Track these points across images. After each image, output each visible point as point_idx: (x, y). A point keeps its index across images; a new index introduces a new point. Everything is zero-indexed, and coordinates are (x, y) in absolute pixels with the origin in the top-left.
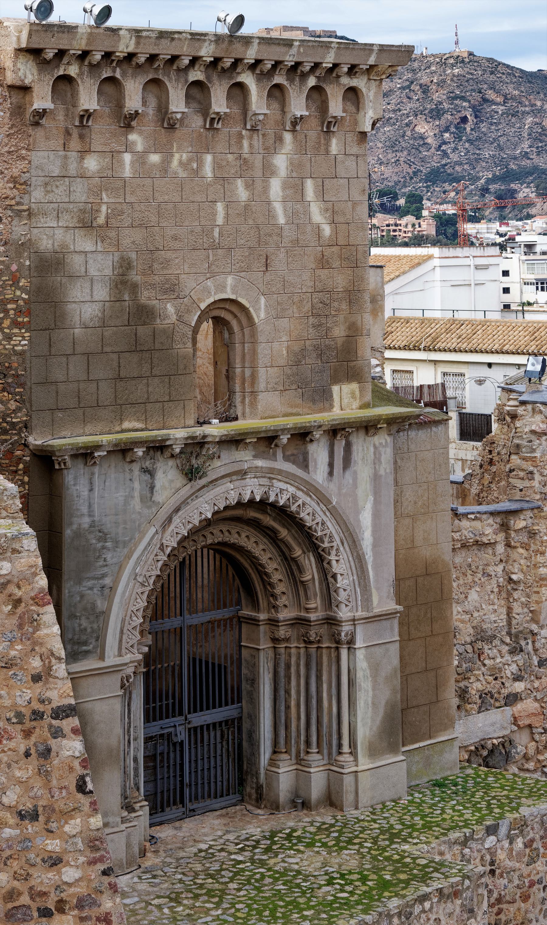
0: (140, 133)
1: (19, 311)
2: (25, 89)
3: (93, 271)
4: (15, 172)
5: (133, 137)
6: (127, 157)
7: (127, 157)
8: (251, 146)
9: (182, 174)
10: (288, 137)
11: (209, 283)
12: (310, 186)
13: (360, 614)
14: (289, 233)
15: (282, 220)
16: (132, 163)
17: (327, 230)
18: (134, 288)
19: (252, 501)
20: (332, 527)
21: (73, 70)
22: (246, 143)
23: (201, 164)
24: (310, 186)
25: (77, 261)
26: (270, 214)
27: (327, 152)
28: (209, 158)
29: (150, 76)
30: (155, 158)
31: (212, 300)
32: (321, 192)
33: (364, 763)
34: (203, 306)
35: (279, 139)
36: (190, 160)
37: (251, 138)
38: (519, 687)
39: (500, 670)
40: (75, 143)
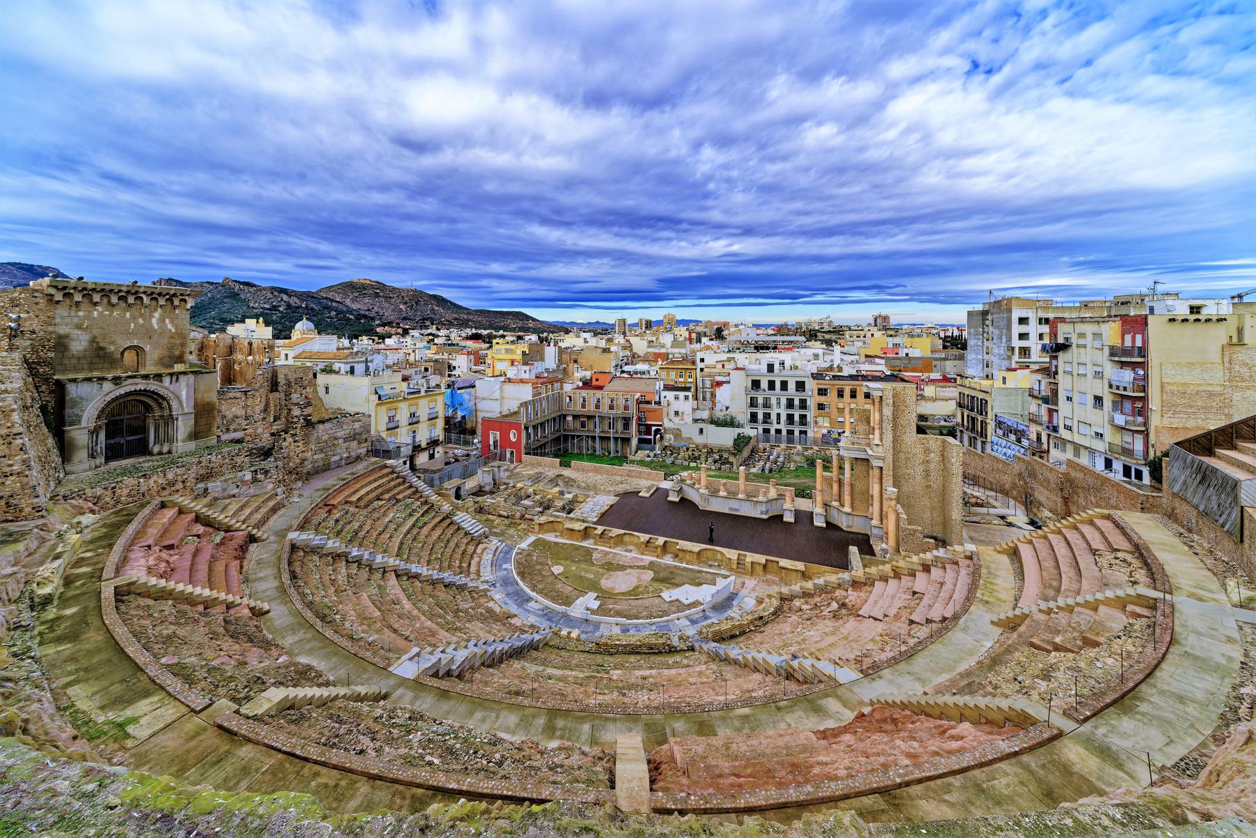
3: (81, 338)
12: (167, 321)
14: (159, 331)
18: (98, 343)
20: (170, 395)
24: (167, 321)
25: (75, 337)
26: (152, 326)
32: (172, 322)
33: (180, 444)
40: (74, 308)
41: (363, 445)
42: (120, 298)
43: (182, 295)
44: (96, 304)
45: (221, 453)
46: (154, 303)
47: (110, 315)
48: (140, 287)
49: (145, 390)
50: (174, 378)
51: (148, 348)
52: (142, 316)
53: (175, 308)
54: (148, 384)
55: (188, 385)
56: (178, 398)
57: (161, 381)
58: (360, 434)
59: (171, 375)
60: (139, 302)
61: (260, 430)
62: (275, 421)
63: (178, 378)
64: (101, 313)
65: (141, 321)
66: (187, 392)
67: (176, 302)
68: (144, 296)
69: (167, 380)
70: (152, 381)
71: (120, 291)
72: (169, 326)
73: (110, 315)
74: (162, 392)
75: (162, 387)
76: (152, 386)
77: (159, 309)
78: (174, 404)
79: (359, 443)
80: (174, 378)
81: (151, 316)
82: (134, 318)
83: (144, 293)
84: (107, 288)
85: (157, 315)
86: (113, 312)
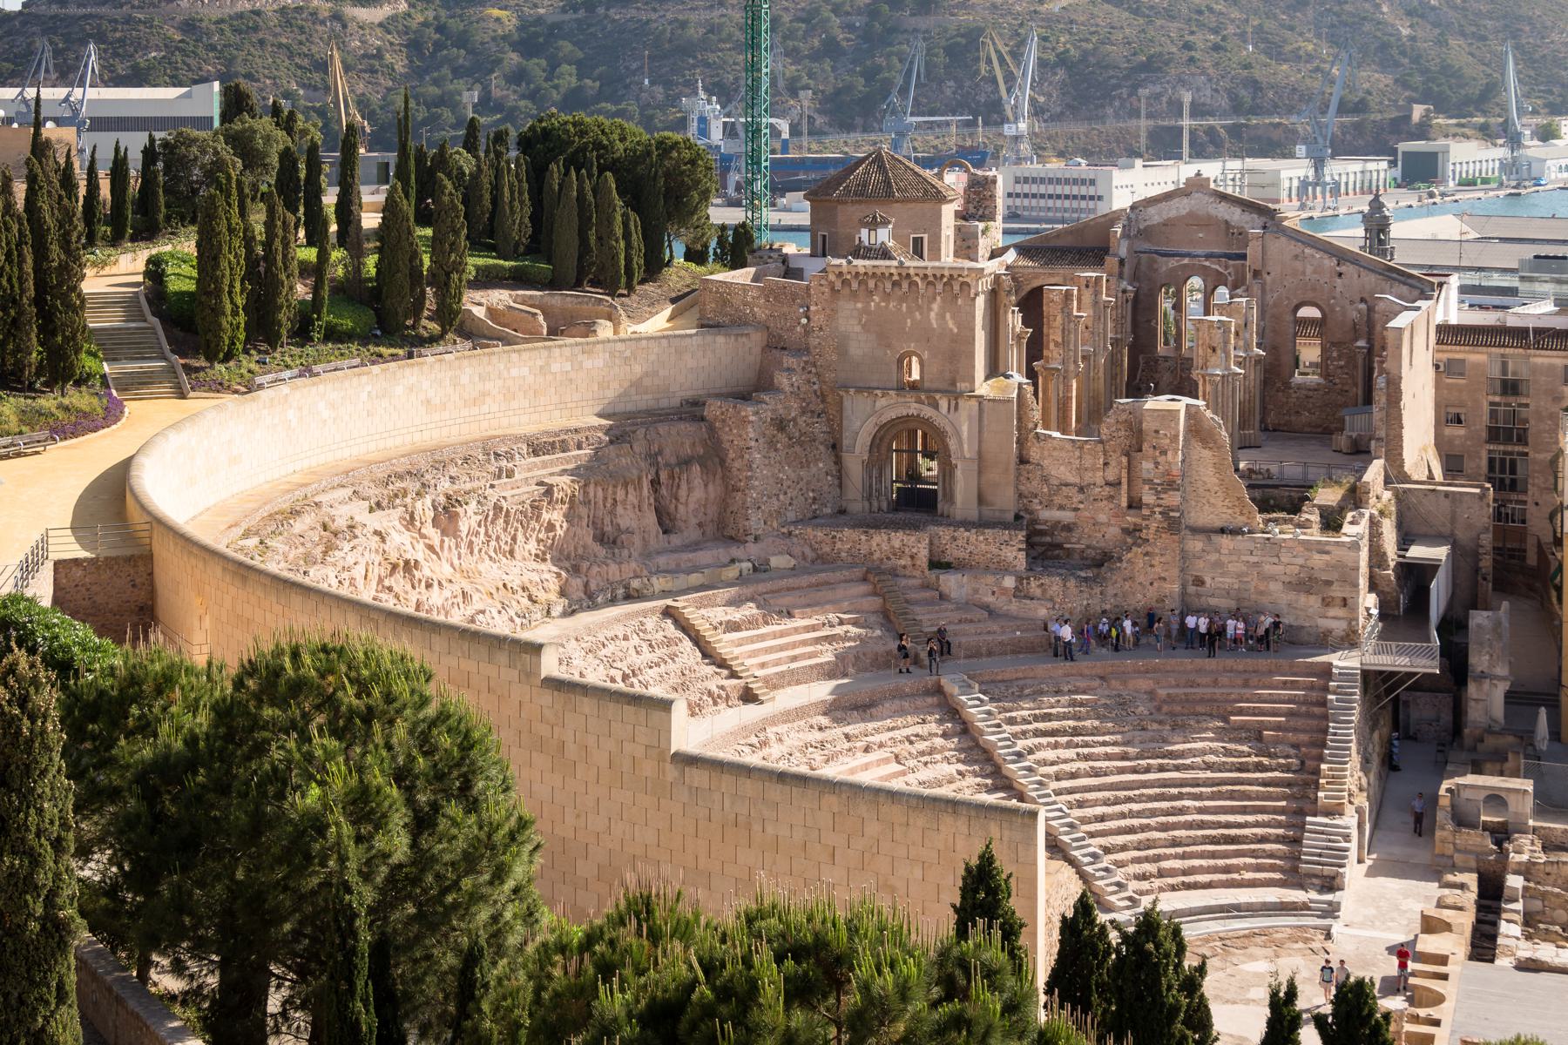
10: (938, 298)
12: (948, 316)
17: (956, 330)
20: (948, 429)
24: (948, 316)
32: (953, 318)
35: (935, 299)
38: (1081, 506)
41: (1333, 612)
42: (895, 284)
45: (983, 534)
46: (931, 288)
48: (908, 268)
49: (918, 415)
52: (919, 308)
55: (970, 417)
56: (958, 434)
58: (1329, 583)
61: (1102, 518)
62: (1130, 507)
64: (877, 305)
65: (918, 315)
67: (956, 287)
68: (917, 279)
71: (891, 274)
72: (951, 324)
79: (1327, 602)
81: (930, 309)
84: (878, 272)
85: (935, 306)
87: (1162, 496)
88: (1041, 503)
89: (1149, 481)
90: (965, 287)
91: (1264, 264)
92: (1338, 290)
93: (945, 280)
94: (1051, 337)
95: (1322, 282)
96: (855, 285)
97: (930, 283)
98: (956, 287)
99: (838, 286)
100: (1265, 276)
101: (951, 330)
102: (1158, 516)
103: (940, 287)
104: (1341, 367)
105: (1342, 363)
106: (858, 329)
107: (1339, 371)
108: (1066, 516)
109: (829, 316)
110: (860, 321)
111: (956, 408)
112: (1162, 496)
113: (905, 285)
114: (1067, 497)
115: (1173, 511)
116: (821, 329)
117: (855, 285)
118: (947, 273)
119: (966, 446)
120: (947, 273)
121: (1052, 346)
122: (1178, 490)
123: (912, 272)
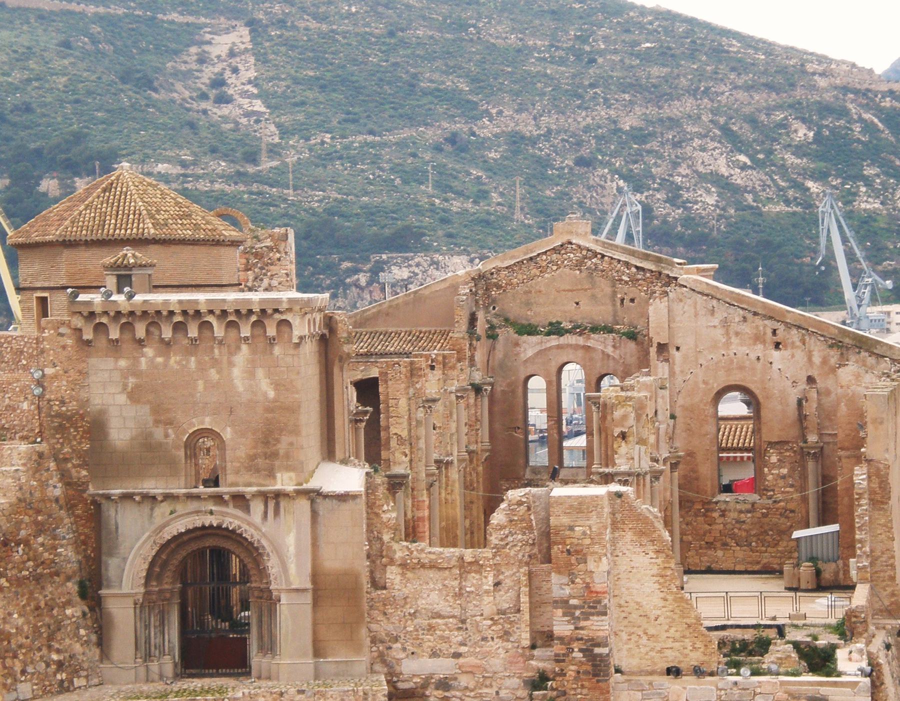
0: (151, 347)
1: (84, 432)
2: (80, 330)
4: (81, 368)
5: (145, 350)
6: (143, 360)
7: (143, 360)
8: (220, 352)
9: (176, 367)
10: (244, 347)
11: (194, 420)
13: (284, 587)
15: (241, 389)
16: (147, 363)
17: (271, 394)
19: (211, 526)
20: (264, 542)
21: (104, 320)
22: (216, 351)
23: (188, 362)
24: (260, 373)
27: (271, 354)
28: (193, 359)
29: (150, 321)
30: (160, 360)
31: (196, 429)
32: (269, 375)
34: (191, 431)
35: (238, 348)
36: (181, 360)
37: (220, 348)
38: (463, 649)
39: (448, 638)
43: (276, 311)
44: (140, 343)
46: (233, 333)
47: (165, 365)
49: (219, 527)
50: (271, 505)
51: (227, 434)
52: (215, 363)
53: (272, 341)
54: (224, 514)
57: (247, 509)
59: (265, 496)
60: (207, 333)
63: (277, 506)
64: (152, 361)
65: (213, 374)
66: (298, 540)
67: (271, 331)
68: (211, 319)
69: (257, 507)
70: (230, 510)
71: (171, 313)
73: (165, 365)
74: (249, 533)
75: (249, 524)
76: (232, 518)
77: (244, 347)
78: (272, 565)
80: (271, 505)
81: (231, 364)
82: (202, 368)
83: (211, 312)
86: (168, 358)
87: (583, 624)
88: (404, 649)
89: (563, 603)
90: (285, 329)
91: (671, 335)
92: (776, 366)
93: (254, 318)
94: (393, 430)
95: (753, 356)
96: (114, 334)
97: (231, 325)
98: (271, 331)
99: (88, 335)
100: (673, 351)
101: (265, 394)
102: (577, 655)
103: (246, 331)
104: (784, 477)
105: (784, 471)
106: (122, 399)
107: (781, 483)
108: (442, 667)
109: (74, 383)
110: (125, 386)
111: (277, 512)
112: (583, 624)
113: (193, 332)
114: (442, 638)
115: (598, 645)
116: (63, 403)
117: (114, 334)
118: (256, 309)
119: (292, 568)
120: (256, 309)
121: (393, 443)
122: (605, 614)
123: (203, 309)
